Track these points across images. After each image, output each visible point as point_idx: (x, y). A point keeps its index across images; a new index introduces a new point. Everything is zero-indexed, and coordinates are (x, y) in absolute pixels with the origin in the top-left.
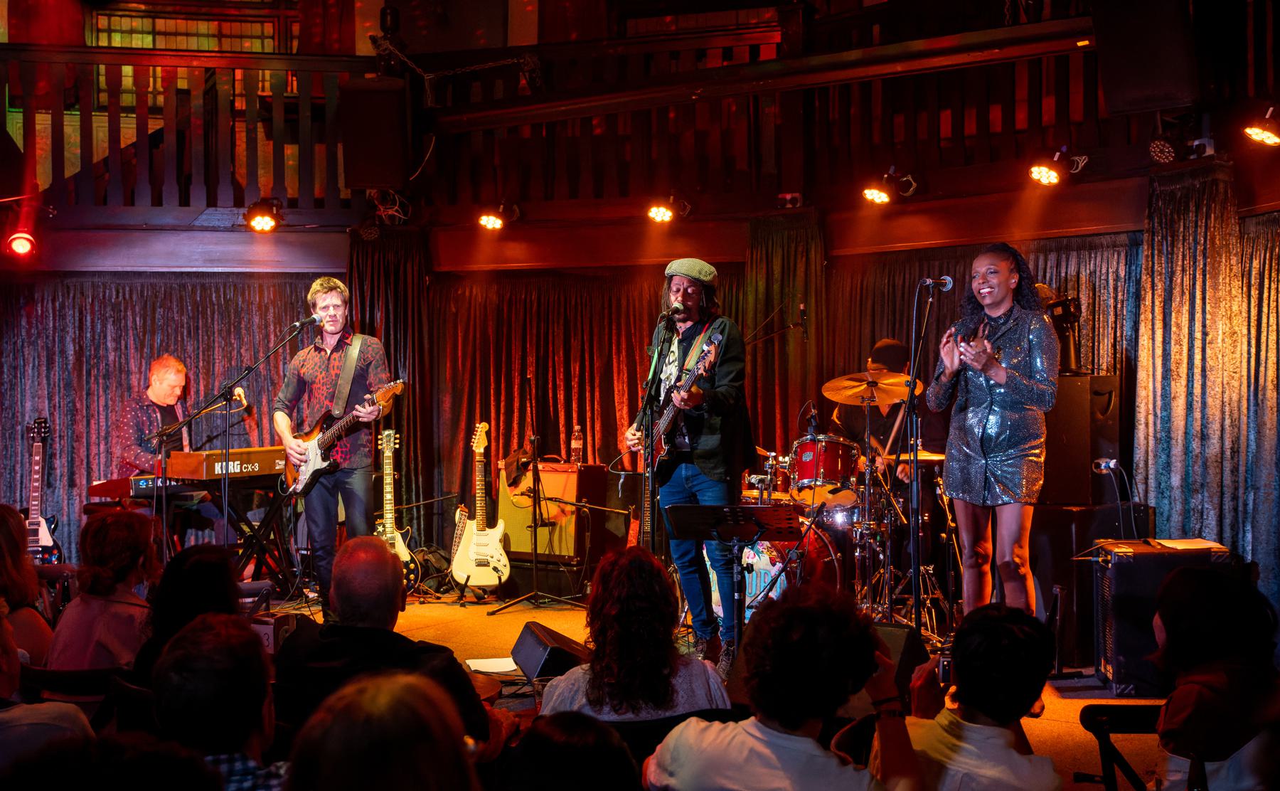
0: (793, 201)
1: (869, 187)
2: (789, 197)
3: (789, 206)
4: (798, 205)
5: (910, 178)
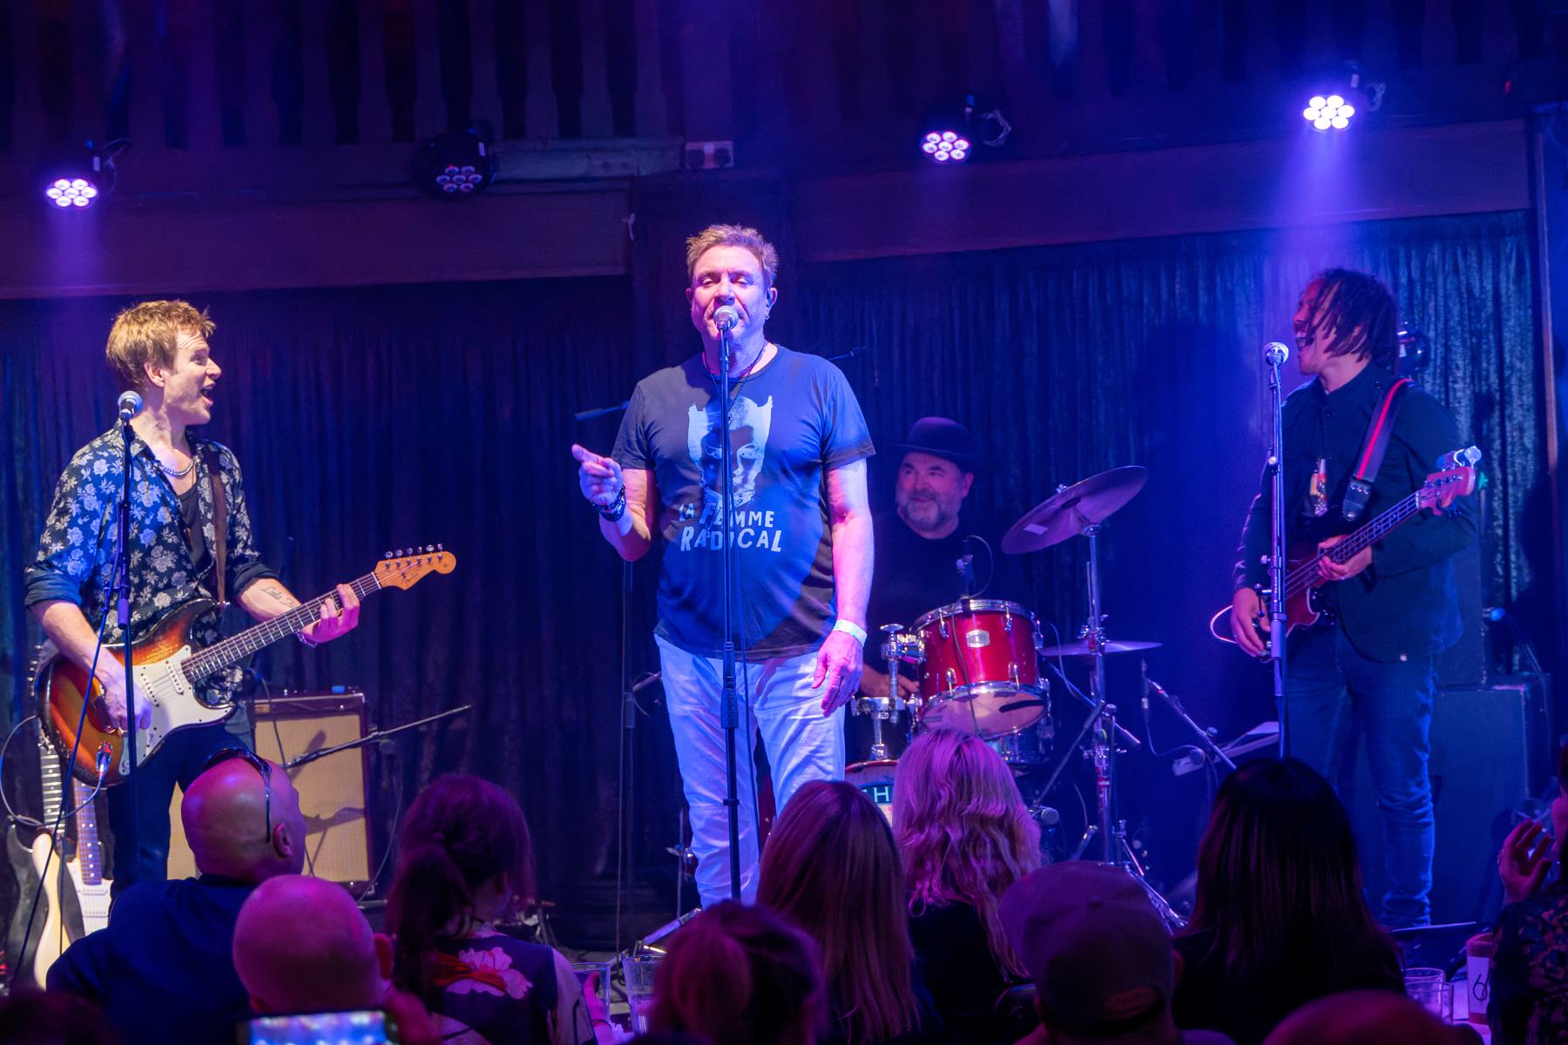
0: (720, 155)
1: (941, 131)
2: (709, 148)
3: (710, 165)
4: (731, 164)
5: (998, 115)
